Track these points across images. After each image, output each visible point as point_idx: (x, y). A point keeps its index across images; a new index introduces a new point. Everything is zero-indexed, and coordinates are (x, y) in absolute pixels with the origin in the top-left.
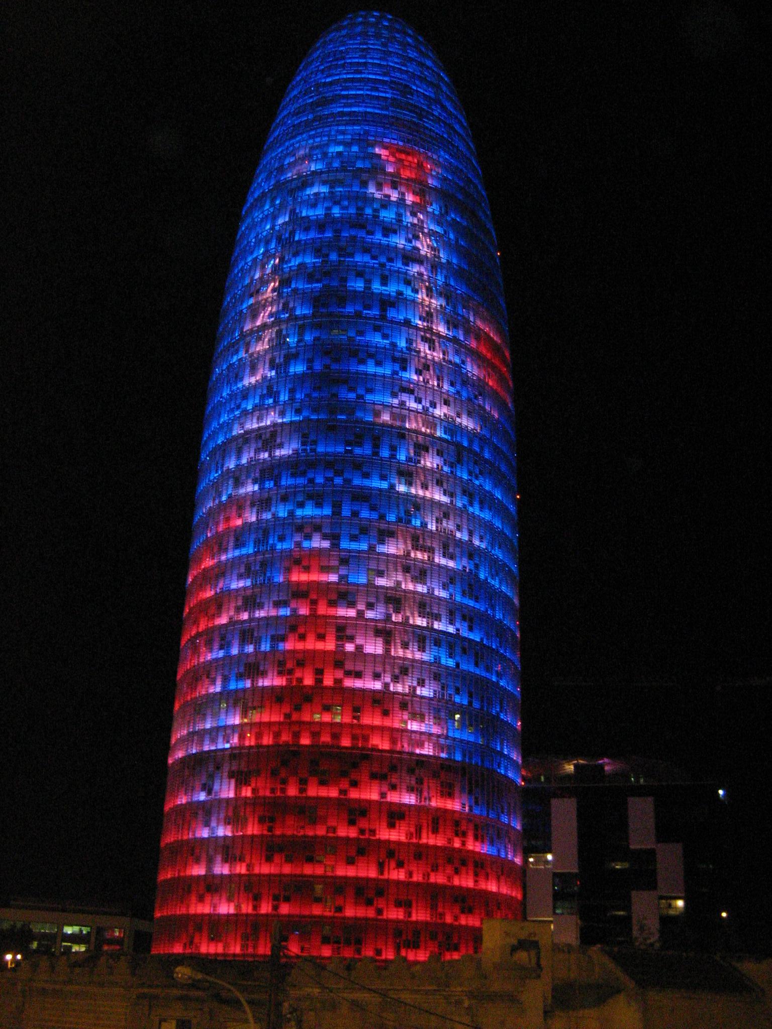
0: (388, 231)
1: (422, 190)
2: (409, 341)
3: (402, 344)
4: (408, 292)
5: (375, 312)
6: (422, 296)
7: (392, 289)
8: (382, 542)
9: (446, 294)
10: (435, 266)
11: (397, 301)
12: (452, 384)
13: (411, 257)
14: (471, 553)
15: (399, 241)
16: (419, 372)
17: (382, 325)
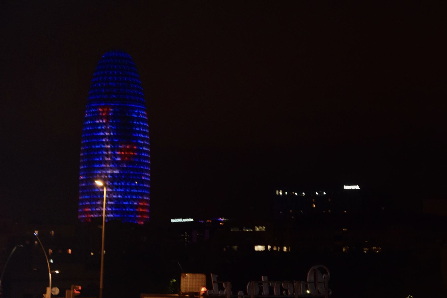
0: (100, 131)
1: (107, 118)
2: (103, 158)
3: (101, 159)
4: (103, 146)
5: (96, 153)
6: (106, 146)
7: (99, 147)
8: (97, 201)
9: (112, 143)
10: (109, 137)
11: (102, 149)
12: (113, 164)
13: (105, 136)
14: (118, 199)
15: (102, 134)
16: (104, 164)
17: (98, 156)
